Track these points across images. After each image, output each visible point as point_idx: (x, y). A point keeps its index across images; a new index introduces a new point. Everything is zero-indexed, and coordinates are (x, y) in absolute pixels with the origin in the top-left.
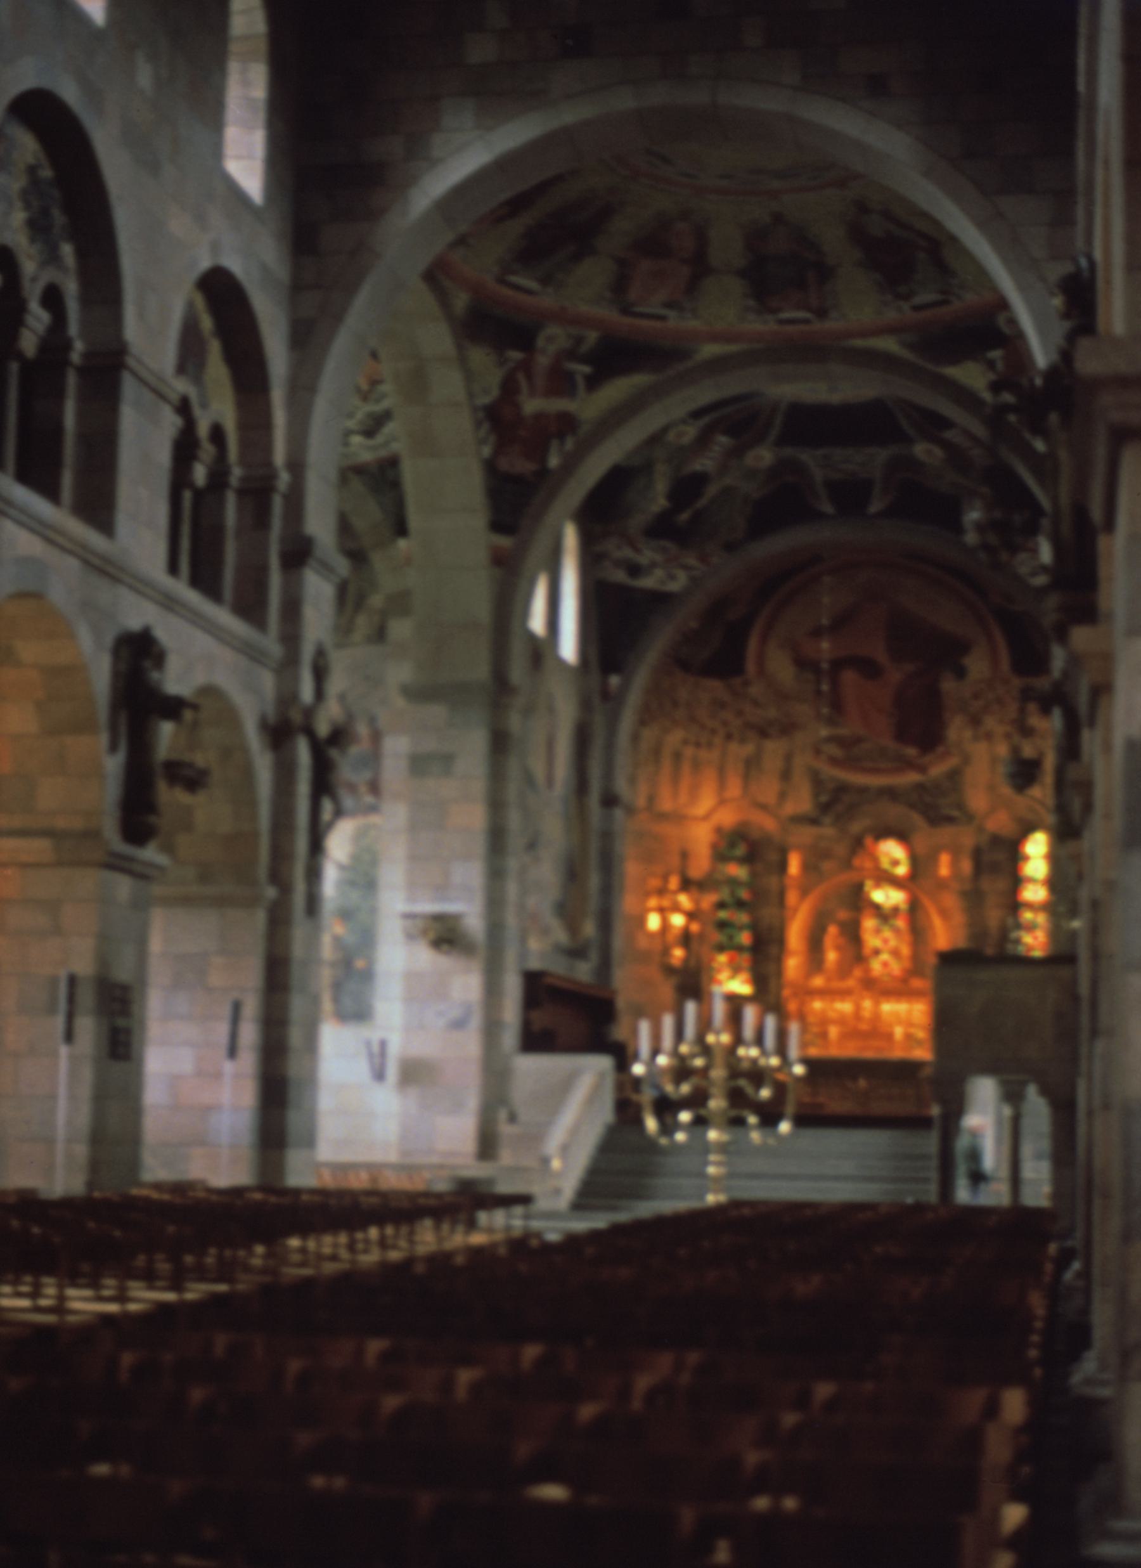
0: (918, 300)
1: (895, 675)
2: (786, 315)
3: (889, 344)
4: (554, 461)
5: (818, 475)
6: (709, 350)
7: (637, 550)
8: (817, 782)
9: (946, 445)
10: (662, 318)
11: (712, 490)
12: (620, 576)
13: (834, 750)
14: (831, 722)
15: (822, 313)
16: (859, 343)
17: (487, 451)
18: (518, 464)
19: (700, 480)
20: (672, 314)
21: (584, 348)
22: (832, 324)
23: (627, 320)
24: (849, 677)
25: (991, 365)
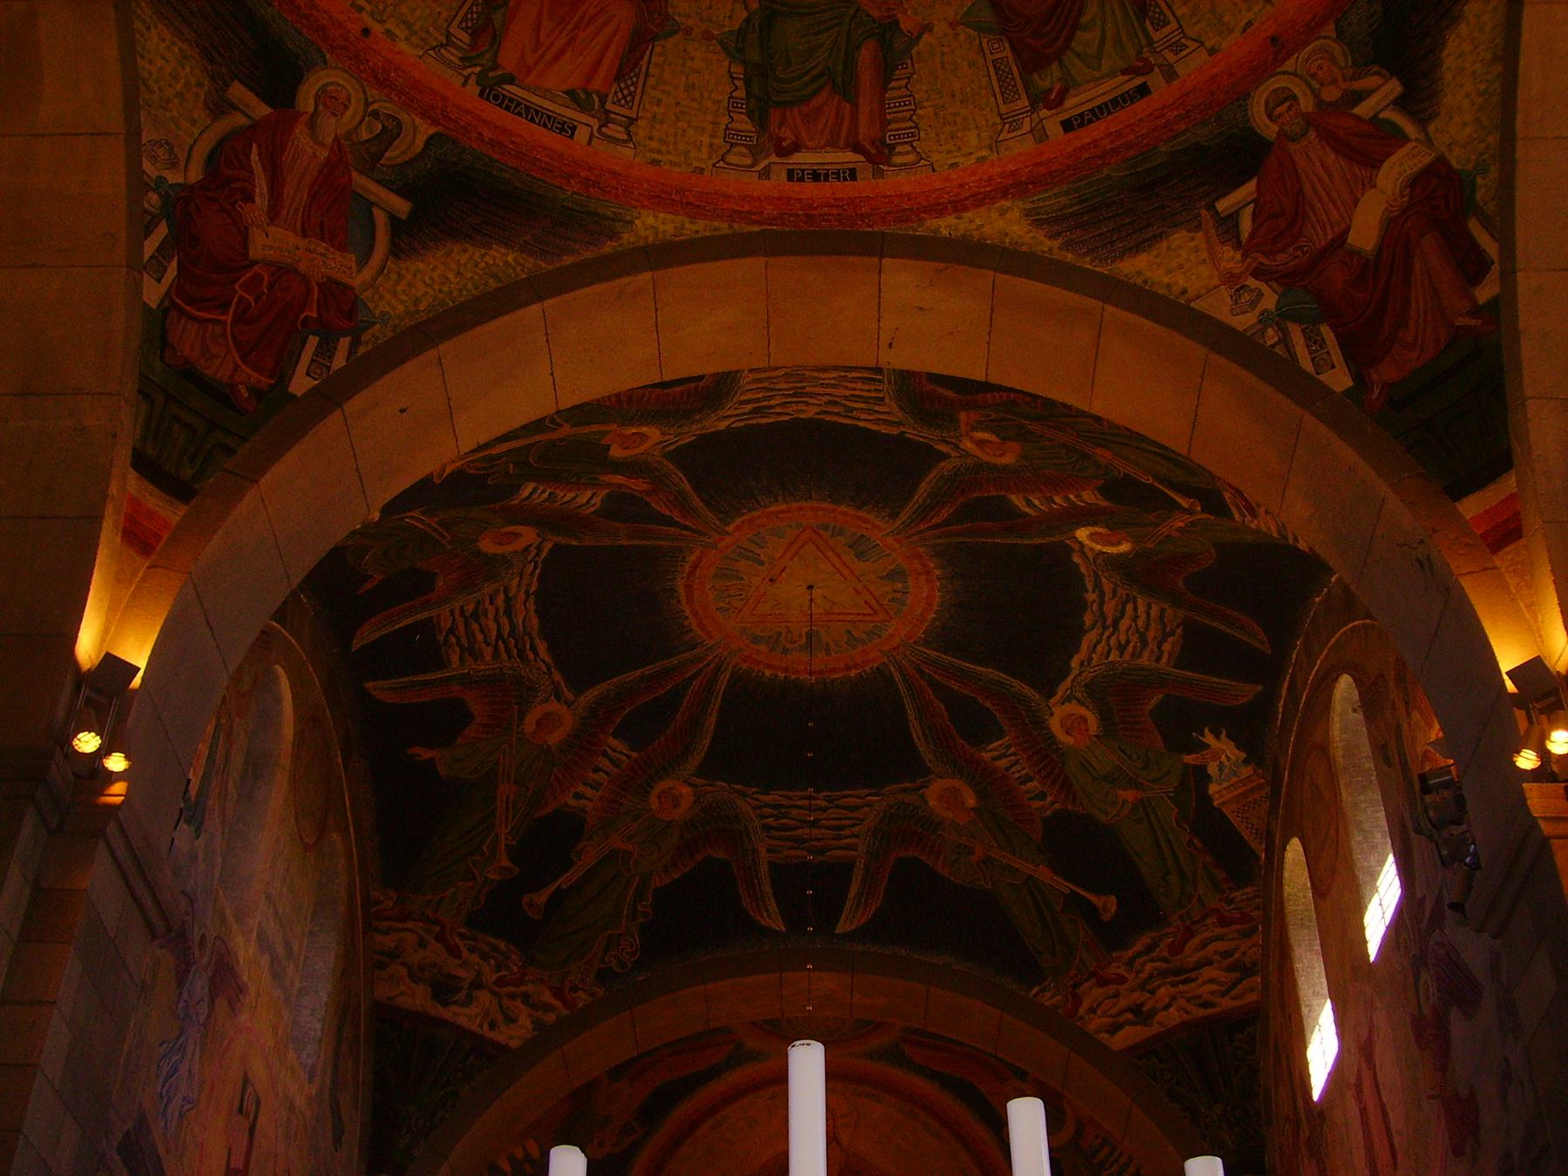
0: (1075, 104)
2: (803, 159)
4: (301, 384)
6: (652, 224)
7: (454, 952)
10: (568, 129)
12: (417, 998)
15: (879, 155)
17: (153, 293)
18: (223, 366)
20: (586, 124)
21: (395, 154)
22: (898, 180)
23: (493, 112)
25: (1229, 225)
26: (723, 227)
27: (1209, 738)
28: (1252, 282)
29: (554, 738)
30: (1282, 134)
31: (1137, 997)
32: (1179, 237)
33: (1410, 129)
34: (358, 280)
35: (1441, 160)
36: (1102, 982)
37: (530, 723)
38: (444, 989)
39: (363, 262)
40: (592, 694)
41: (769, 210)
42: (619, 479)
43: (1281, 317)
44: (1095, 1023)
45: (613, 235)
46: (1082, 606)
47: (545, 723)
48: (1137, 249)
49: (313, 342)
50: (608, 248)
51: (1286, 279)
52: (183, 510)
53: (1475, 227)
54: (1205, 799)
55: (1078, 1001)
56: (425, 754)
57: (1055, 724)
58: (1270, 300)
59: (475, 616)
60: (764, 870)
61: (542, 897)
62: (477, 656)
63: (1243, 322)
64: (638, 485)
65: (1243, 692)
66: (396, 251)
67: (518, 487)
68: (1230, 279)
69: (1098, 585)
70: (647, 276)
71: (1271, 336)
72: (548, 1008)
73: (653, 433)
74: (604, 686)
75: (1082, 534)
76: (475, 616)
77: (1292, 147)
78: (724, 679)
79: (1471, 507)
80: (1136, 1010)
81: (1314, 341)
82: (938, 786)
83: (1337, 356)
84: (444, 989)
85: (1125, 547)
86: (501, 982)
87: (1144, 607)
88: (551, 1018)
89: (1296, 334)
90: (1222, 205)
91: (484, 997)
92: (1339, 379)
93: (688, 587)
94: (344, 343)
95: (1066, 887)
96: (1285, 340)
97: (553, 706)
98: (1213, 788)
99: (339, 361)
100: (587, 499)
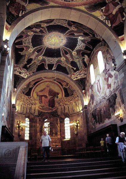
1: (49, 97)
3: (83, 8)
4: (20, 15)
5: (47, 63)
7: (21, 70)
8: (39, 111)
9: (66, 58)
11: (33, 62)
12: (18, 74)
13: (40, 107)
14: (40, 104)
16: (77, 7)
18: (13, 13)
19: (31, 60)
24: (43, 98)
26: (58, 5)
27: (85, 56)
28: (103, 16)
29: (31, 52)
30: (108, 3)
31: (76, 76)
32: (97, 11)
33: (120, 4)
34: (25, 6)
35: (122, 7)
36: (74, 75)
37: (29, 51)
38: (20, 73)
39: (26, 4)
40: (35, 48)
41: (62, 4)
42: (41, 28)
43: (106, 19)
44: (72, 78)
45: (48, 4)
46: (77, 44)
47: (30, 50)
48: (93, 12)
49: (21, 11)
50: (47, 6)
51: (106, 16)
52: (10, 26)
53: (124, 13)
54: (84, 61)
55: (71, 76)
56: (20, 52)
57: (73, 54)
58: (105, 18)
59: (26, 40)
60: (47, 64)
61: (29, 66)
62: (25, 44)
63: (102, 19)
64: (43, 29)
65: (89, 52)
66: (29, 3)
67: (33, 28)
68: (101, 15)
69: (79, 42)
70: (51, 9)
71: (104, 21)
72: (28, 75)
73: (45, 24)
74: (36, 47)
75: (79, 37)
76: (26, 40)
77: (109, 4)
78: (46, 48)
79: (120, 37)
80: (76, 77)
81: (108, 22)
82: (62, 58)
83: (110, 23)
84: (20, 73)
85: (83, 39)
86: (25, 73)
87: (83, 44)
88: (29, 76)
89: (106, 21)
90: (102, 9)
91: (23, 74)
92: (110, 25)
93: (45, 39)
94: (24, 11)
95: (72, 67)
96: (105, 21)
97: (31, 49)
98: (85, 60)
99: (23, 13)
100: (38, 30)
